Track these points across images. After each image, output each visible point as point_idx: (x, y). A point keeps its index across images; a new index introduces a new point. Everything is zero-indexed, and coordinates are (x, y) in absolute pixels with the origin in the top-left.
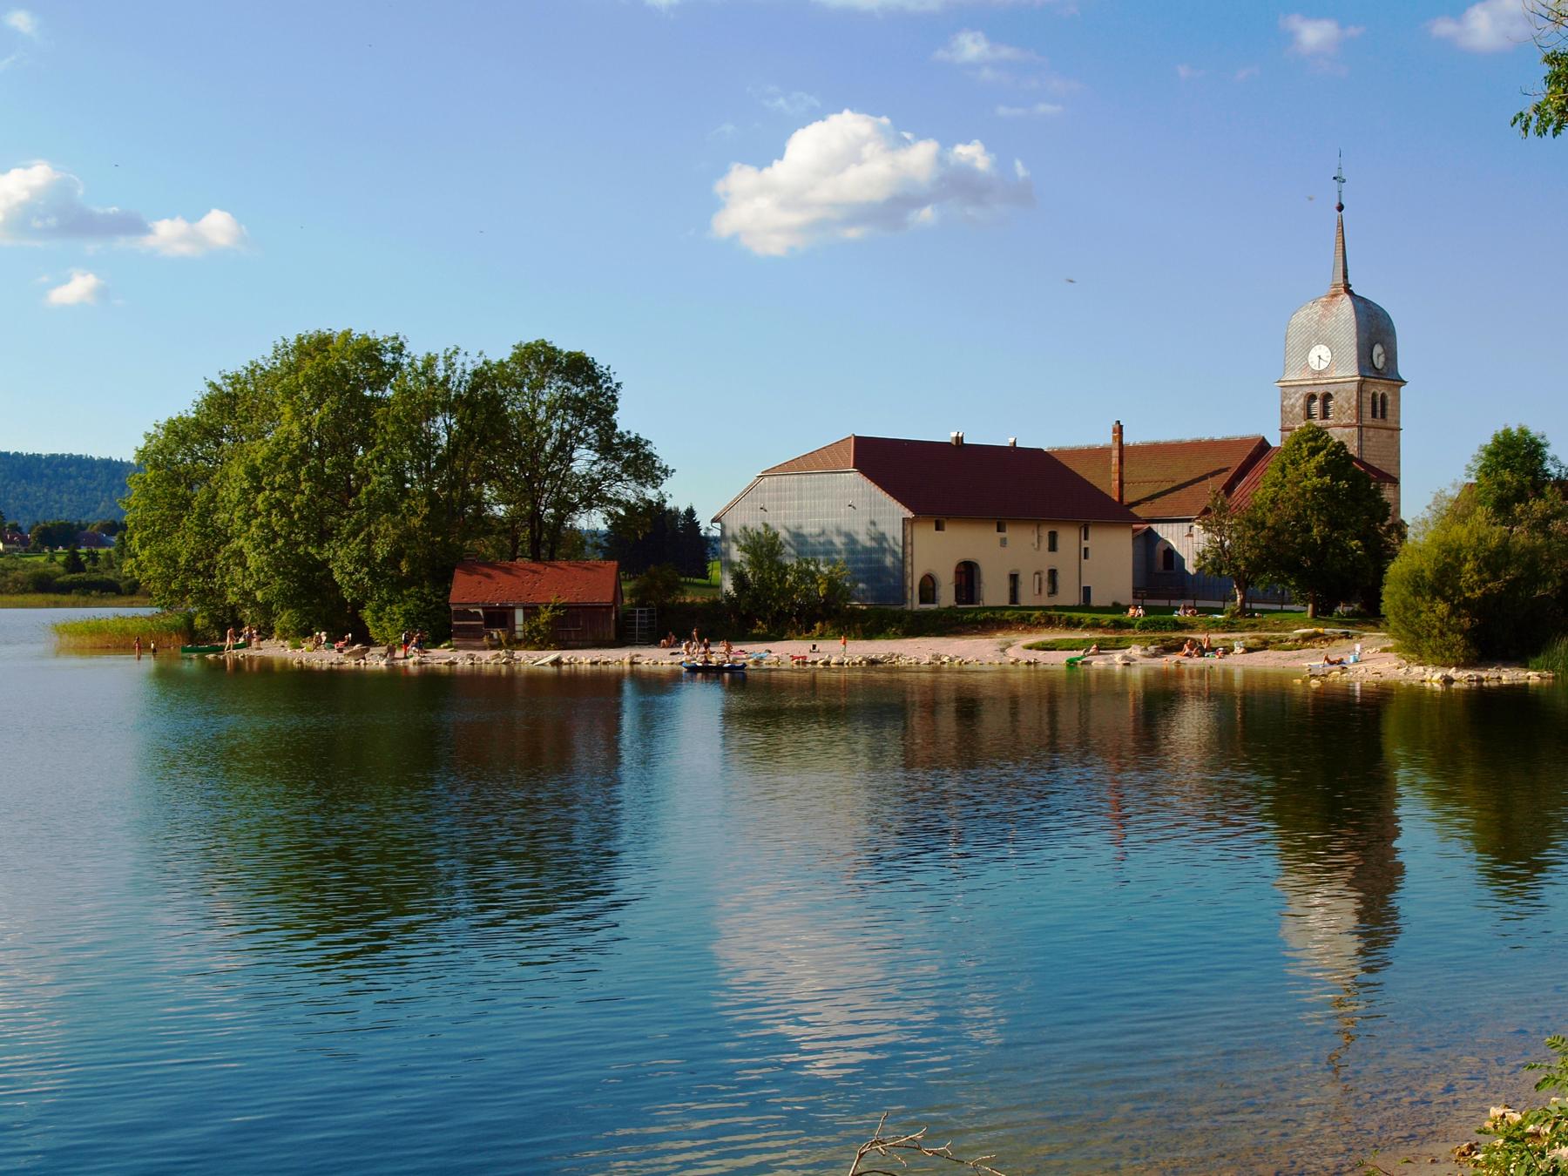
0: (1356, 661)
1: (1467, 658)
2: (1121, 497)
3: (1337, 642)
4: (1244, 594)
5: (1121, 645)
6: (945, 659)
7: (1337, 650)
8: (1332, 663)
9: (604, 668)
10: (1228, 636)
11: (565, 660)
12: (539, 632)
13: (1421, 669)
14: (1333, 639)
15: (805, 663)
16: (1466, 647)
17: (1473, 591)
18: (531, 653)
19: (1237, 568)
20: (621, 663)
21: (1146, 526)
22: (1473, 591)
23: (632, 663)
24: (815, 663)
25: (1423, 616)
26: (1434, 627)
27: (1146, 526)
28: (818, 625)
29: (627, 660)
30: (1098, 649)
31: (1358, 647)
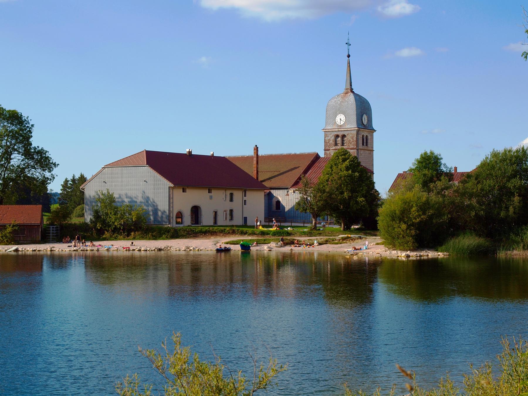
0: (366, 249)
1: (413, 247)
2: (257, 178)
3: (356, 241)
4: (316, 220)
5: (266, 242)
6: (192, 248)
7: (358, 244)
8: (357, 249)
9: (38, 252)
10: (310, 238)
11: (20, 249)
12: (6, 237)
13: (395, 251)
14: (355, 240)
15: (129, 250)
16: (413, 242)
17: (416, 219)
18: (3, 246)
19: (313, 209)
20: (46, 251)
21: (268, 191)
22: (416, 219)
23: (51, 251)
24: (134, 250)
25: (396, 229)
26: (400, 234)
27: (268, 191)
28: (132, 233)
29: (49, 249)
30: (257, 244)
31: (367, 243)
